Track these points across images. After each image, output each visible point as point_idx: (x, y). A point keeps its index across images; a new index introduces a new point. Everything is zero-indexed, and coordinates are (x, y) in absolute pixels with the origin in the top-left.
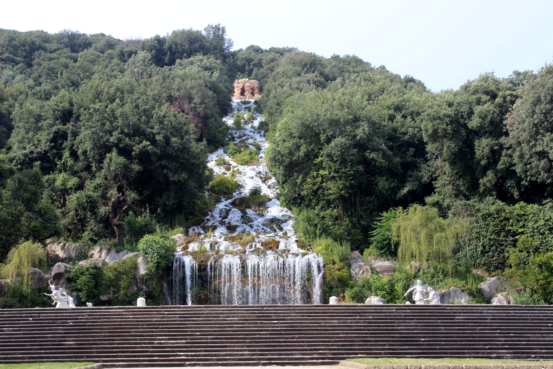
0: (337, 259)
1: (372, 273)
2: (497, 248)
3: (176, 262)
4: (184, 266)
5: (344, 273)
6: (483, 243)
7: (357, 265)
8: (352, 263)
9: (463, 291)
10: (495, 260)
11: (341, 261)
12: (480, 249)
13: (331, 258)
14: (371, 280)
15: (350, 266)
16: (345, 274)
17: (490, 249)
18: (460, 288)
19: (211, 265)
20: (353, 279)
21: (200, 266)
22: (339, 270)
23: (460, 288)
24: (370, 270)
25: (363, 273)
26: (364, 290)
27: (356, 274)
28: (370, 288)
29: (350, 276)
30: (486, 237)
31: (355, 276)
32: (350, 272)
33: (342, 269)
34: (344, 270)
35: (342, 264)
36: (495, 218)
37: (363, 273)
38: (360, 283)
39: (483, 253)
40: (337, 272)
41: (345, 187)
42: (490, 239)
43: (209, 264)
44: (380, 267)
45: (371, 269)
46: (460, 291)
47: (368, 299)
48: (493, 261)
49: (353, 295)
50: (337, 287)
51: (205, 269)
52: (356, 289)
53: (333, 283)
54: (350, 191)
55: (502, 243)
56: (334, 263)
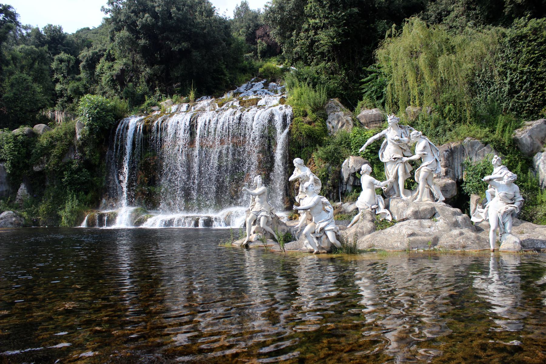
0: (309, 110)
1: (355, 125)
2: (532, 84)
3: (122, 124)
4: (127, 128)
5: (317, 127)
6: (512, 80)
7: (335, 116)
8: (328, 113)
9: (486, 144)
10: (529, 102)
11: (313, 112)
12: (506, 88)
13: (302, 109)
14: (352, 134)
15: (325, 117)
16: (317, 128)
17: (522, 87)
18: (480, 139)
19: (158, 126)
20: (330, 135)
21: (145, 127)
22: (310, 123)
23: (480, 139)
24: (351, 122)
25: (342, 126)
26: (342, 149)
27: (333, 127)
28: (349, 146)
29: (325, 131)
30: (515, 70)
31: (332, 130)
32: (325, 126)
33: (315, 122)
34: (316, 123)
35: (314, 116)
36: (530, 41)
37: (342, 126)
38: (338, 139)
39: (512, 93)
40: (306, 126)
41: (338, 35)
42: (522, 73)
43: (155, 124)
44: (365, 116)
45: (353, 120)
46: (481, 144)
47: (346, 161)
48: (526, 103)
49: (325, 156)
50: (307, 146)
51: (150, 131)
52: (331, 147)
53: (300, 141)
54: (344, 39)
55: (541, 76)
56: (305, 115)
